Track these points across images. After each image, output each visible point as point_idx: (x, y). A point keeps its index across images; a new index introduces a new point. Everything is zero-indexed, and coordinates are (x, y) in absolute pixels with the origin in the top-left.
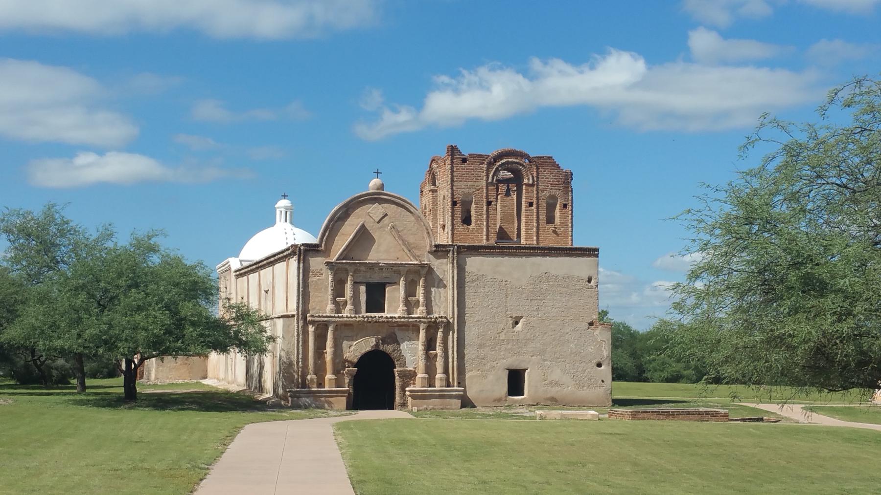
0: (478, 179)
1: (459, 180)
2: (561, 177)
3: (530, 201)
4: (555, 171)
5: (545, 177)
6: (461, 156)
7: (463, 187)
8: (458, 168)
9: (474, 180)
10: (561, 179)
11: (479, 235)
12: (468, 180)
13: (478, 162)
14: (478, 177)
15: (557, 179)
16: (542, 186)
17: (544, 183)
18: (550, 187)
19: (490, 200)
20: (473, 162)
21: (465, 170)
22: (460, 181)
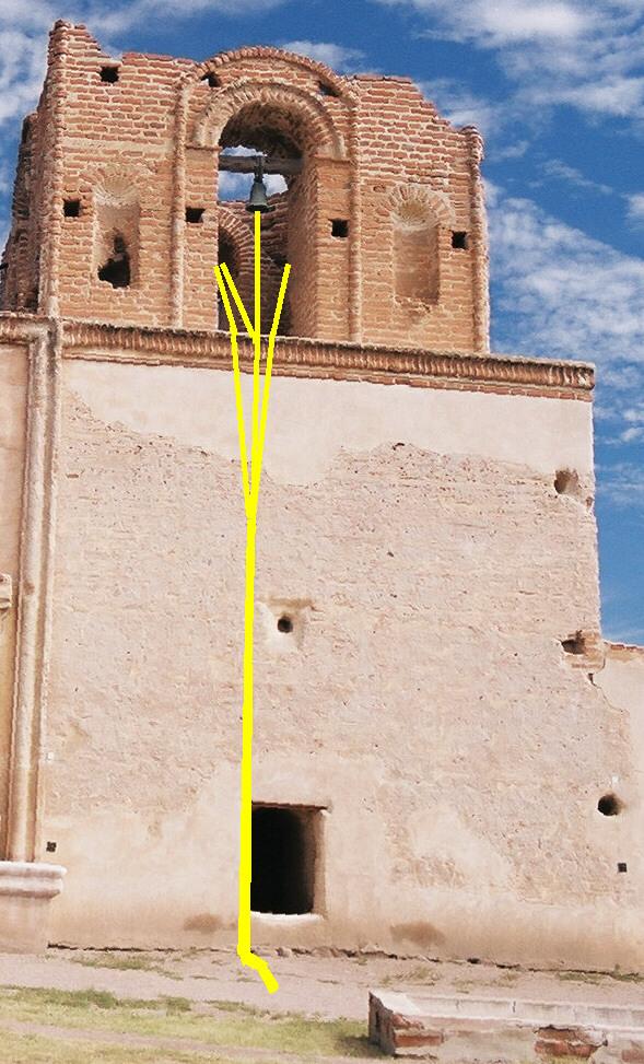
0: (155, 135)
1: (88, 132)
2: (441, 146)
3: (336, 216)
4: (417, 126)
5: (386, 143)
6: (94, 59)
7: (102, 155)
8: (88, 94)
9: (142, 135)
10: (444, 151)
11: (154, 315)
12: (117, 136)
13: (155, 81)
14: (153, 126)
15: (427, 150)
16: (376, 169)
17: (384, 161)
18: (402, 174)
19: (194, 204)
20: (140, 79)
21: (111, 104)
22: (92, 137)
